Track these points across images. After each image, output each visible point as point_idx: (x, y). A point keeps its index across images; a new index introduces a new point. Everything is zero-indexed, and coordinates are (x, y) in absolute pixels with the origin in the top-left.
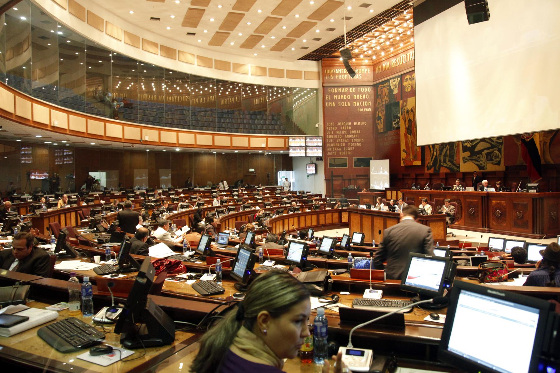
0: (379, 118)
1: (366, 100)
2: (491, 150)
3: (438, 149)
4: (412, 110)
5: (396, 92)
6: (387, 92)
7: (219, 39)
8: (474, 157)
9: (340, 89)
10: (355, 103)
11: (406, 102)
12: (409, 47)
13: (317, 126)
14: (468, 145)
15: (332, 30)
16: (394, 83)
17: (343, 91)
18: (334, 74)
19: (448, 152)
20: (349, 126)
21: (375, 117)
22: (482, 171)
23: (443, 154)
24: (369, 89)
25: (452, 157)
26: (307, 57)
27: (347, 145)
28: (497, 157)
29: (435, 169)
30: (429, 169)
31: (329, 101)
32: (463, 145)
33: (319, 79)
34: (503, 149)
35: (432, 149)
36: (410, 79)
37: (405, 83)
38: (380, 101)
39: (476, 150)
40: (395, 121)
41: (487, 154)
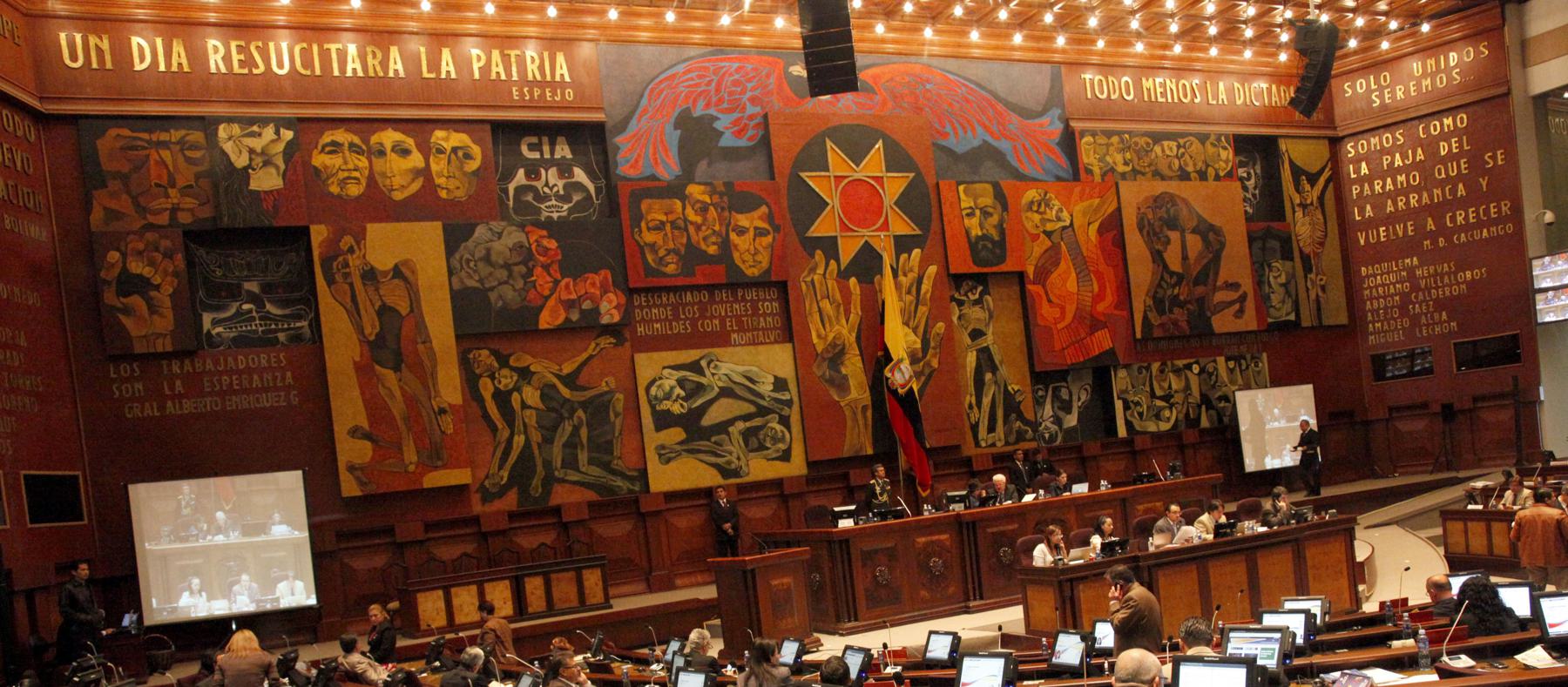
0: (131, 284)
2: (757, 422)
3: (533, 422)
4: (397, 272)
5: (267, 181)
6: (186, 175)
11: (360, 236)
14: (676, 409)
16: (258, 144)
19: (584, 432)
22: (738, 481)
25: (602, 450)
28: (776, 440)
32: (653, 407)
35: (500, 424)
36: (352, 145)
37: (319, 160)
38: (124, 204)
39: (706, 421)
40: (218, 308)
41: (747, 435)
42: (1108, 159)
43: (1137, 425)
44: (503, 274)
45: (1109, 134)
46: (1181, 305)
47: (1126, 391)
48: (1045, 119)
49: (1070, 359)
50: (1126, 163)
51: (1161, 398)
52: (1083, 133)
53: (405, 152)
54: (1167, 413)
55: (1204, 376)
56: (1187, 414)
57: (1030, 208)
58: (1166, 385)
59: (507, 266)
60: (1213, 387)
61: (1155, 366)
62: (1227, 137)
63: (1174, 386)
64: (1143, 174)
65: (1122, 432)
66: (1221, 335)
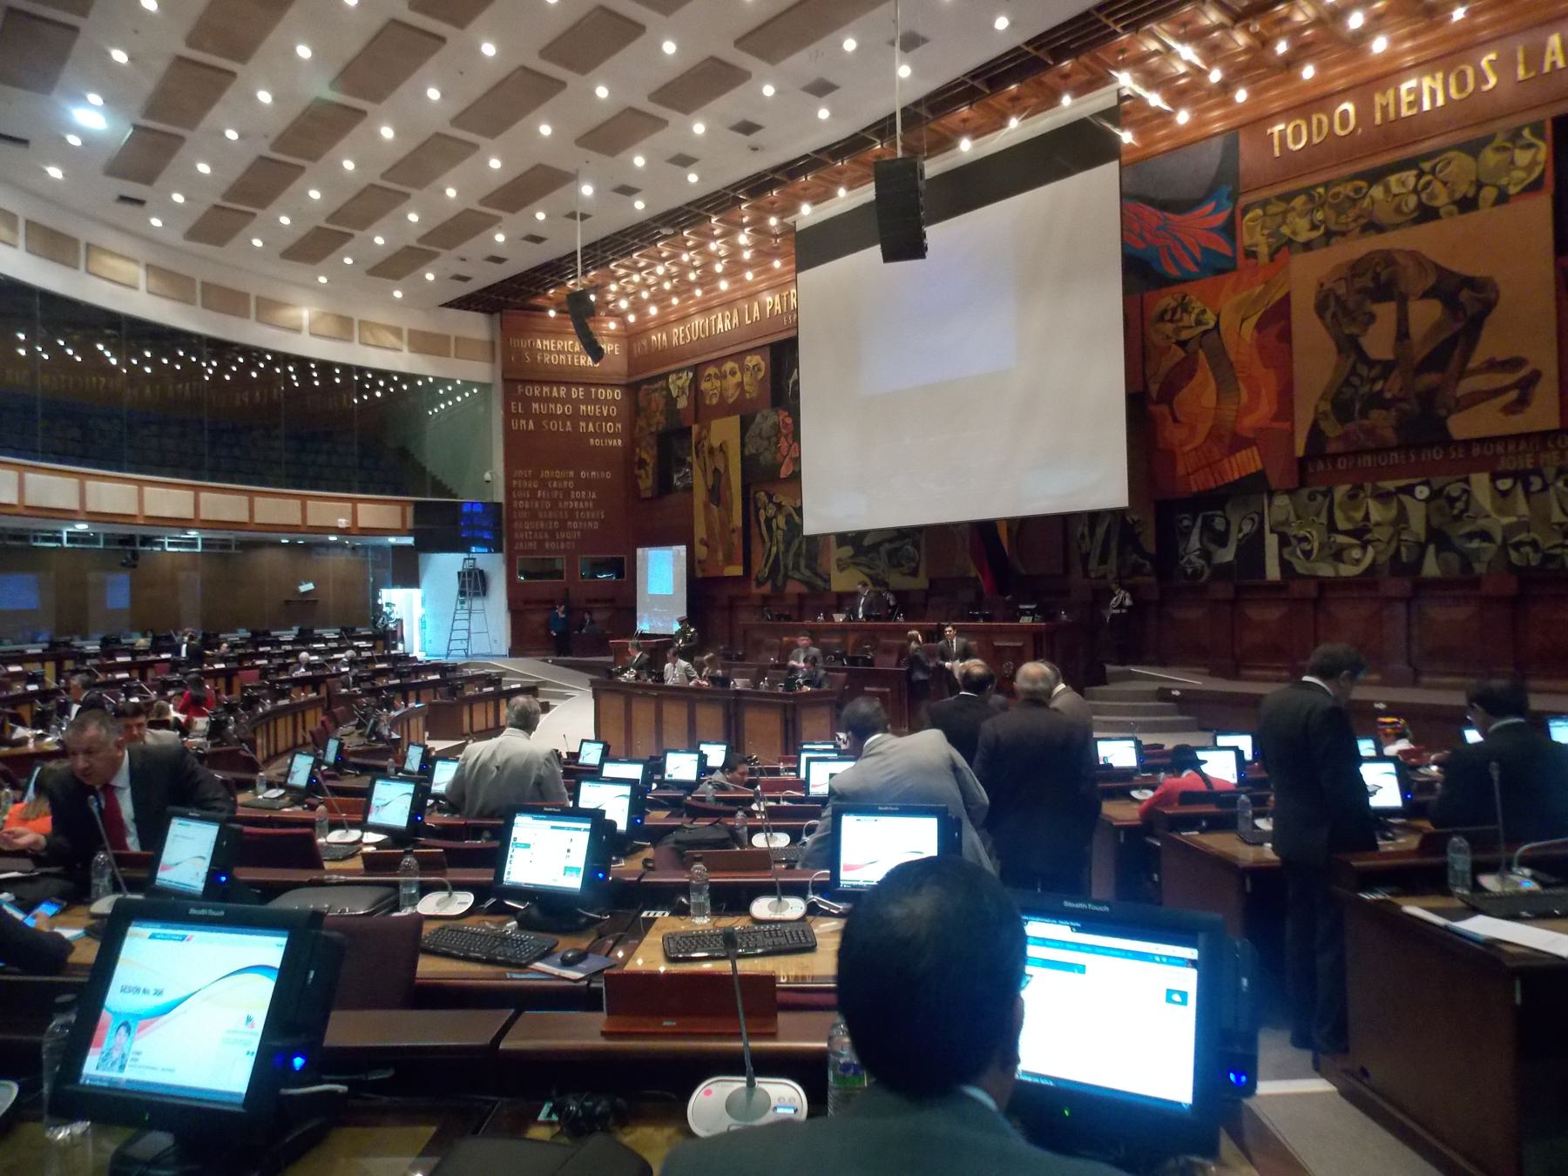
0: (642, 463)
1: (609, 418)
5: (682, 403)
6: (662, 402)
7: (217, 225)
8: (863, 559)
9: (546, 389)
10: (582, 424)
11: (709, 430)
12: (714, 303)
13: (487, 476)
15: (537, 239)
16: (680, 383)
17: (555, 394)
18: (533, 350)
20: (568, 479)
21: (629, 461)
23: (793, 550)
24: (618, 394)
26: (464, 303)
27: (563, 527)
29: (774, 585)
30: (760, 584)
31: (518, 416)
33: (493, 361)
34: (923, 542)
37: (705, 386)
41: (890, 554)
42: (1285, 230)
43: (1300, 566)
44: (765, 443)
45: (1287, 197)
46: (1386, 405)
47: (1287, 523)
48: (1209, 207)
49: (1197, 484)
50: (1314, 227)
51: (1346, 533)
52: (1245, 211)
53: (733, 373)
54: (1356, 553)
55: (1442, 502)
56: (1397, 555)
57: (1161, 318)
58: (1359, 515)
59: (769, 438)
60: (1458, 518)
61: (1341, 491)
62: (1537, 130)
63: (1375, 516)
64: (1343, 234)
65: (1273, 572)
66: (1468, 443)
